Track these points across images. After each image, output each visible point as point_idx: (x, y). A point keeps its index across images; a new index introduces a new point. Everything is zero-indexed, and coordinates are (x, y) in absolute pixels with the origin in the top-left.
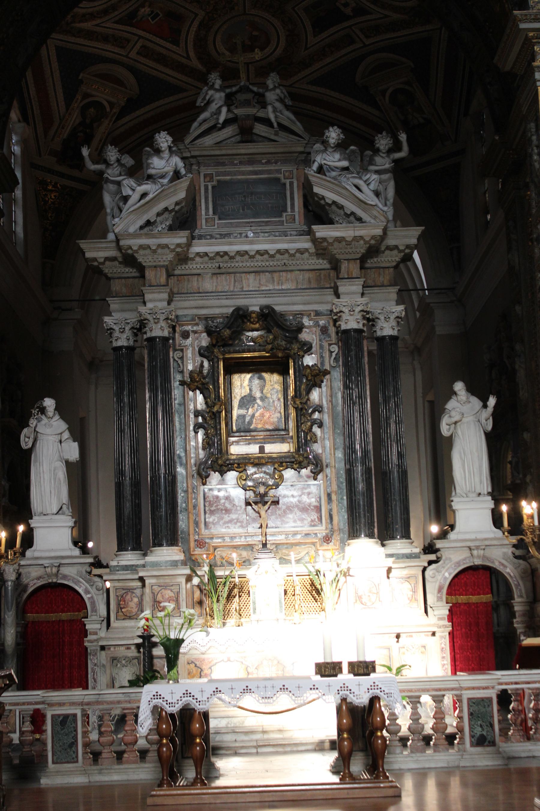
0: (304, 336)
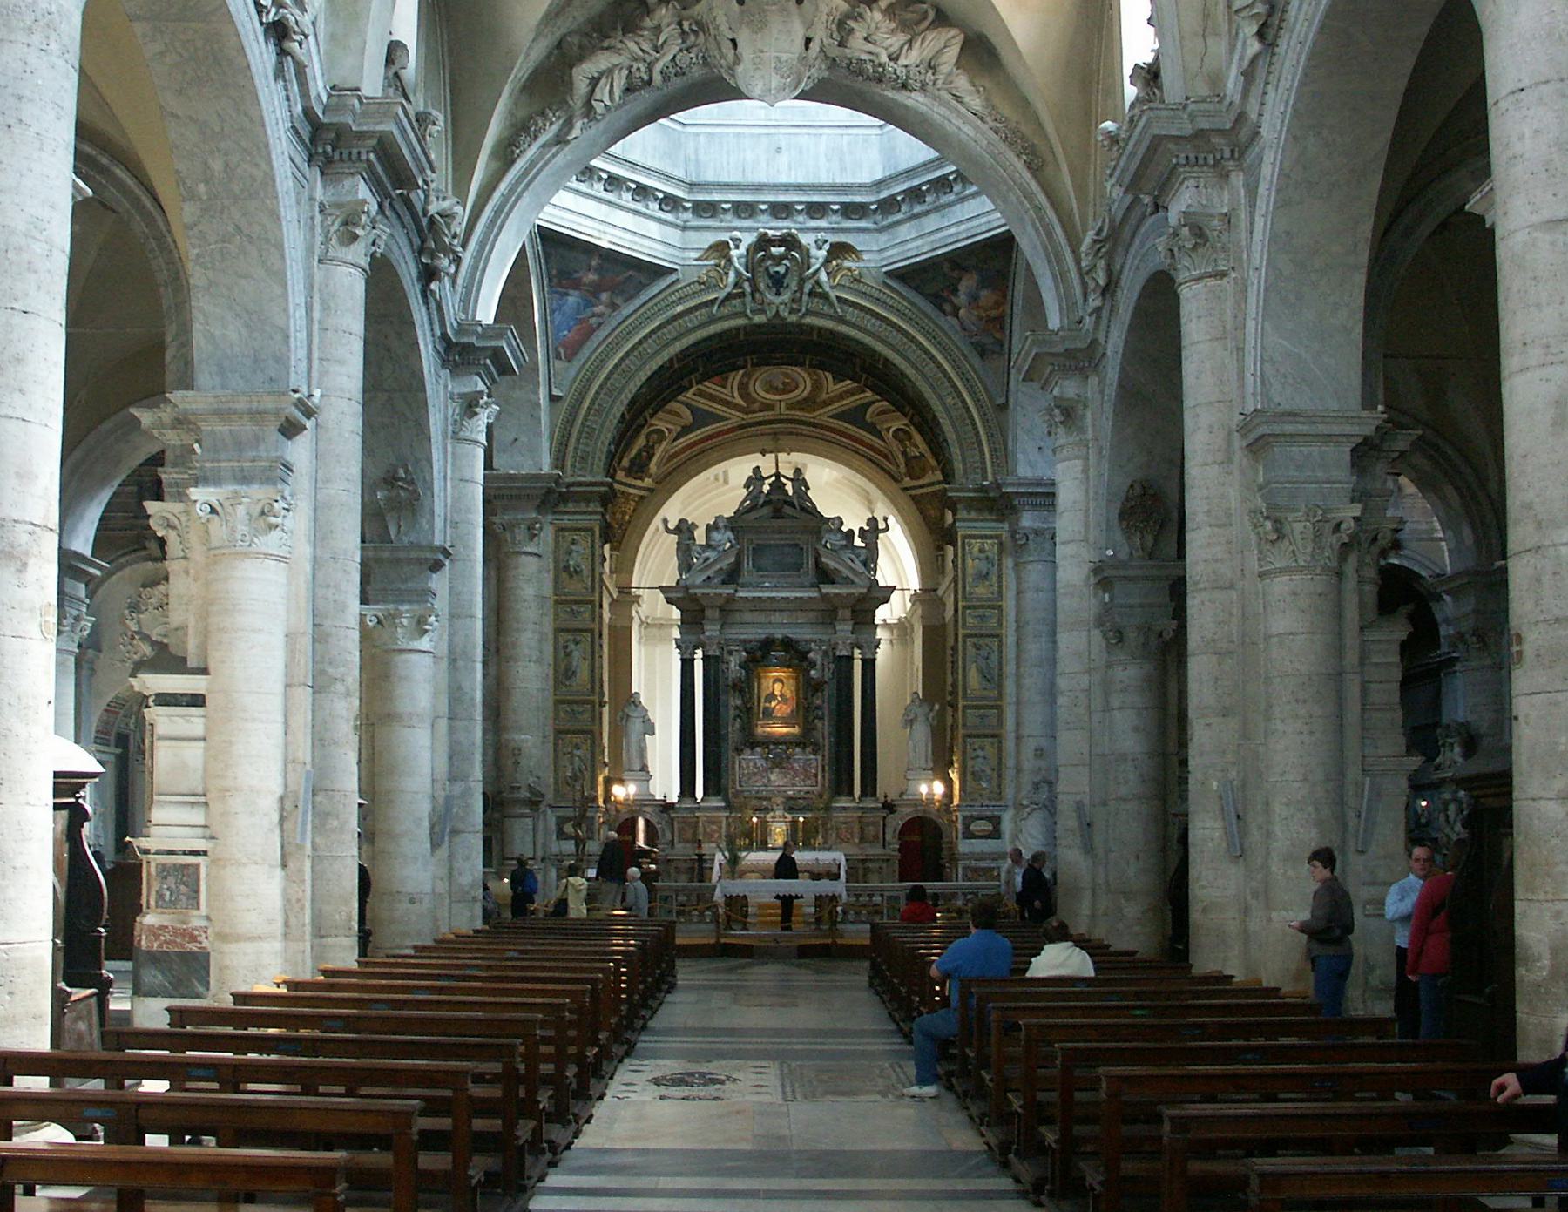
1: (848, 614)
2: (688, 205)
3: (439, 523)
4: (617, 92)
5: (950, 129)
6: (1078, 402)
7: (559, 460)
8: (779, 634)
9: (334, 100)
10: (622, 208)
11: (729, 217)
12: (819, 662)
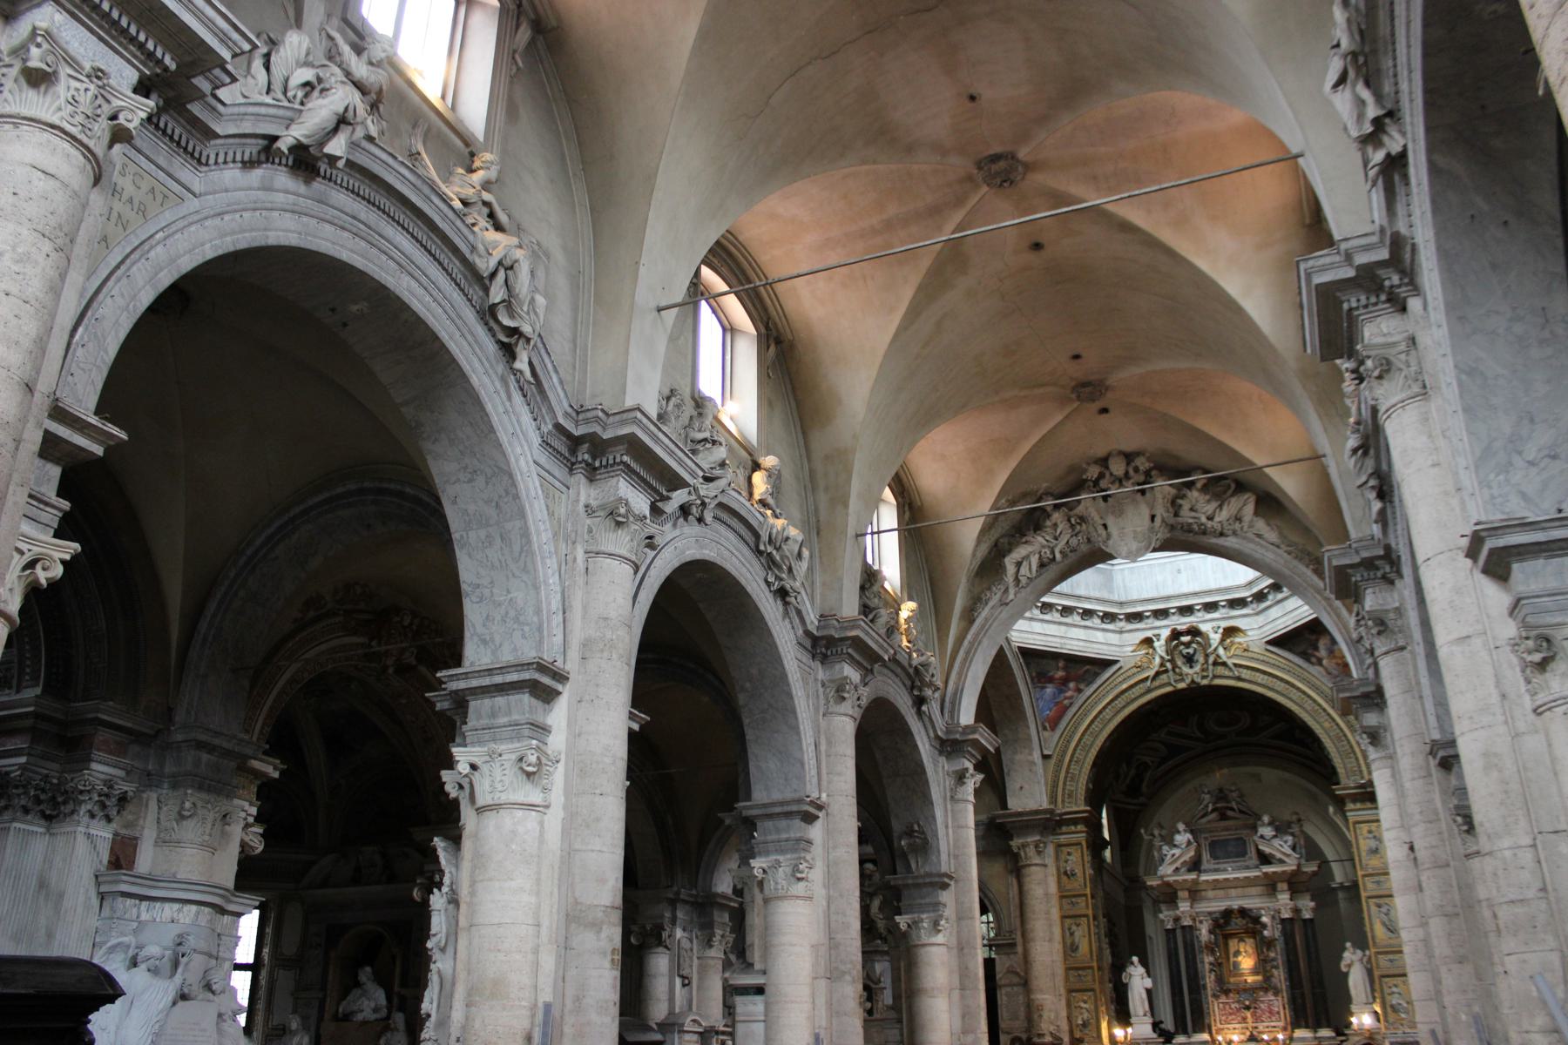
0: (1264, 919)
1: (1285, 886)
2: (1122, 617)
3: (944, 857)
4: (1034, 567)
5: (1257, 556)
6: (1379, 727)
7: (1053, 798)
8: (1235, 904)
9: (822, 623)
10: (1075, 626)
11: (1150, 621)
12: (1269, 924)
